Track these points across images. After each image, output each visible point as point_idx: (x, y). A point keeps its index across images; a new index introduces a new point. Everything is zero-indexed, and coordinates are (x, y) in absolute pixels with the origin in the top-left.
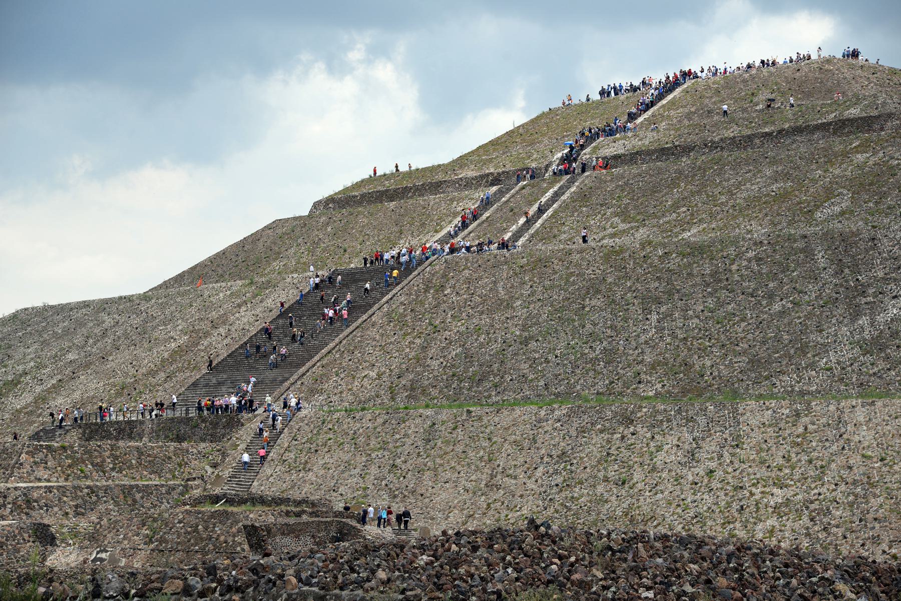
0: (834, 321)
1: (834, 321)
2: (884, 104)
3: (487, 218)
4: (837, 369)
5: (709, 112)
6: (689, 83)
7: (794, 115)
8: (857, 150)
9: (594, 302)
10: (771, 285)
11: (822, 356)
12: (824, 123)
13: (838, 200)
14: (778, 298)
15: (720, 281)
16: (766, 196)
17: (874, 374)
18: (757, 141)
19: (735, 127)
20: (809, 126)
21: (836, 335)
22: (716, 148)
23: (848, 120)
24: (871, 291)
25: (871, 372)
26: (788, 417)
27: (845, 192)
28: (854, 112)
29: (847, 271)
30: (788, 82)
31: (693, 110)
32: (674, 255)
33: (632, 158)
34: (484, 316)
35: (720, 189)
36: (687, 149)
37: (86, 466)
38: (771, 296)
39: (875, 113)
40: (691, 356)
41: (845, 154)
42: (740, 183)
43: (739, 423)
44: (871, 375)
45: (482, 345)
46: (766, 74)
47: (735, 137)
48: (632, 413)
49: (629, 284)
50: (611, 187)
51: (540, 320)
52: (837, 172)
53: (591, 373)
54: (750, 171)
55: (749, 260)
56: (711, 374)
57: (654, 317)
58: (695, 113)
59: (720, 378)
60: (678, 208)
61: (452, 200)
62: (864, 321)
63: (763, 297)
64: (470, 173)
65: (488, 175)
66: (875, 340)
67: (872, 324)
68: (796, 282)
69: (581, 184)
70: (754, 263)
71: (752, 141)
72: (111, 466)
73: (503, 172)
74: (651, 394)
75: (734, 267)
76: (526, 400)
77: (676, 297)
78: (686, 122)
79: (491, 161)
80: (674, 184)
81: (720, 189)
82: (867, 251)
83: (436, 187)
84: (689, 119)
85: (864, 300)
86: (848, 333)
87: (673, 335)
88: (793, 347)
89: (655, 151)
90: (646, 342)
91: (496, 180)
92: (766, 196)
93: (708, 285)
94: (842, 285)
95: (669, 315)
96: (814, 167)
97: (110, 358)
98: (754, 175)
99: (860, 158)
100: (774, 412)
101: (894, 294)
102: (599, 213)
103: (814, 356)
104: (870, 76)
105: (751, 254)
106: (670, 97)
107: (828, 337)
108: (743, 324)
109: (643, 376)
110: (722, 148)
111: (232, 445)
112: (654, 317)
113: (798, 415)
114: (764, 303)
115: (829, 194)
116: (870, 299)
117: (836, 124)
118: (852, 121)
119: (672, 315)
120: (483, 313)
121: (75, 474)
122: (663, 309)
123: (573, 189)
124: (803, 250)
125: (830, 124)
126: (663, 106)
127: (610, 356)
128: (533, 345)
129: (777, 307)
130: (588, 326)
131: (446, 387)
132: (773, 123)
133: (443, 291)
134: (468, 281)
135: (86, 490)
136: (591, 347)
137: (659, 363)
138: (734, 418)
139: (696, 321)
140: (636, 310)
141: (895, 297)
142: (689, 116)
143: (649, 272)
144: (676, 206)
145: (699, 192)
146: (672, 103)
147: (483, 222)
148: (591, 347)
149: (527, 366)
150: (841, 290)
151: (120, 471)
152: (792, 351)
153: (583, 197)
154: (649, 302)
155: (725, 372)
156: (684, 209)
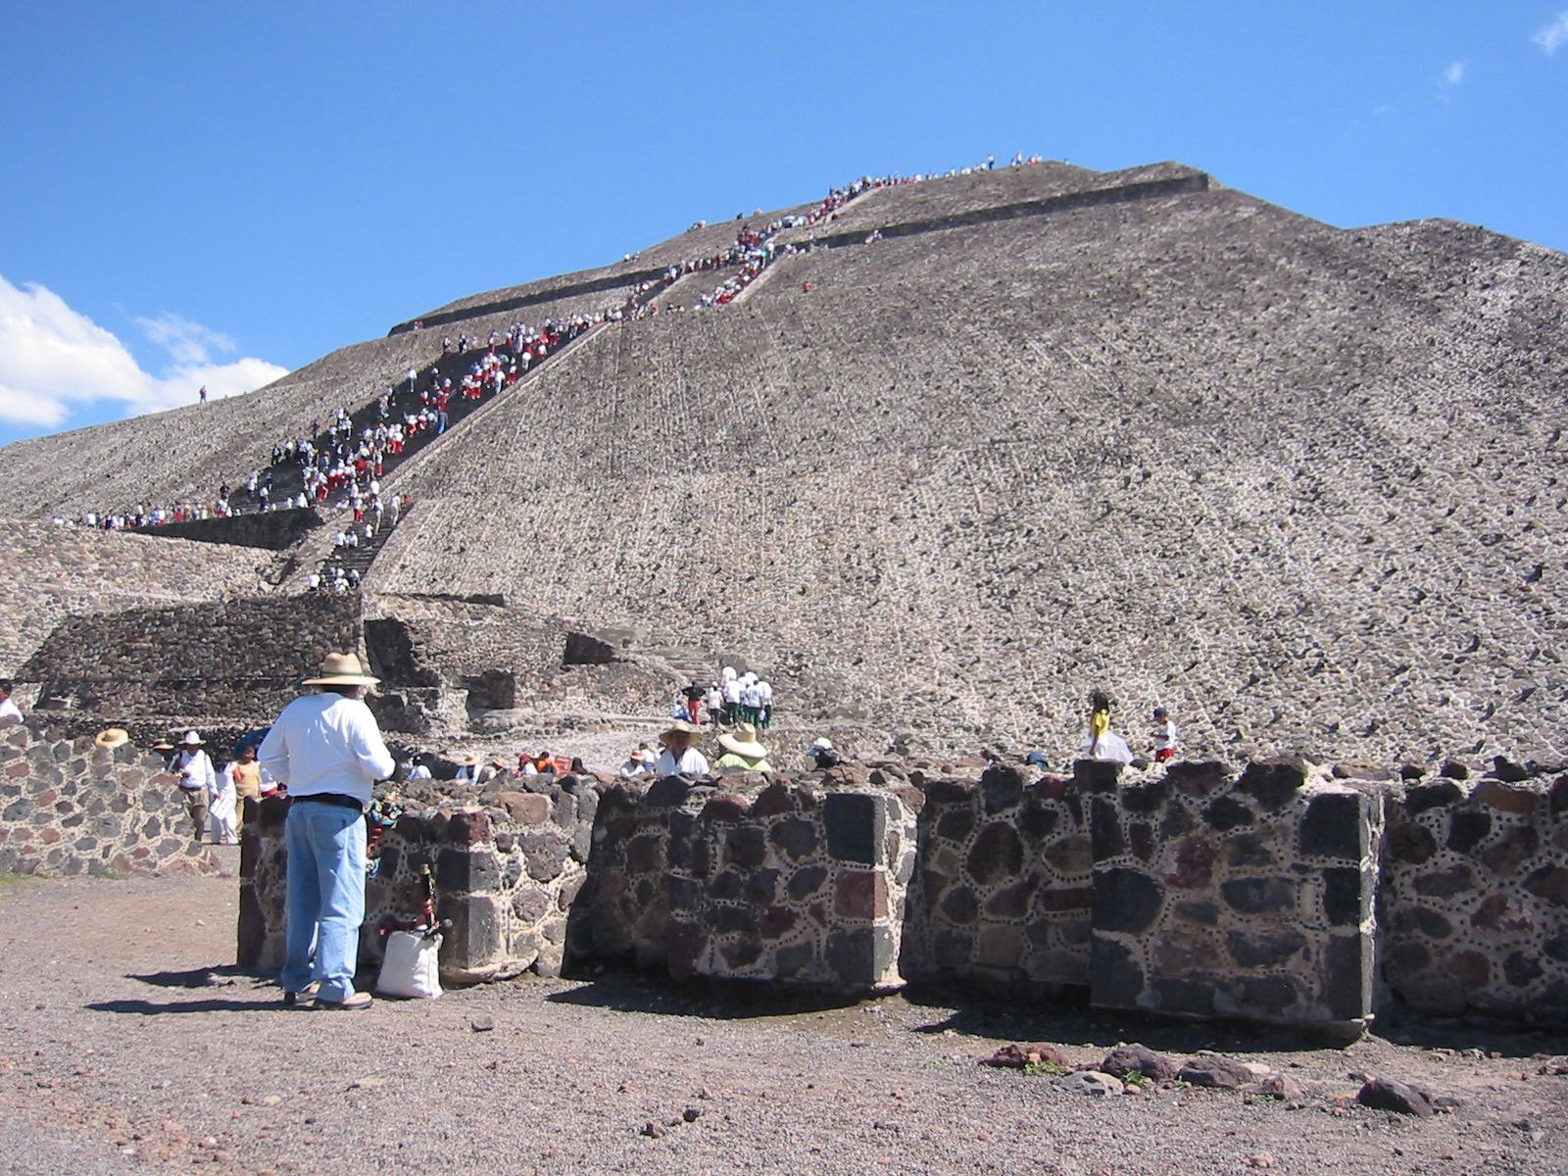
23: (1143, 184)
37: (50, 561)
45: (724, 405)
52: (1165, 230)
61: (588, 301)
72: (96, 567)
83: (564, 293)
93: (1109, 305)
95: (1065, 339)
97: (117, 476)
111: (306, 550)
121: (30, 573)
125: (1118, 189)
135: (45, 598)
140: (995, 341)
151: (112, 577)
154: (1014, 333)
155: (1242, 395)
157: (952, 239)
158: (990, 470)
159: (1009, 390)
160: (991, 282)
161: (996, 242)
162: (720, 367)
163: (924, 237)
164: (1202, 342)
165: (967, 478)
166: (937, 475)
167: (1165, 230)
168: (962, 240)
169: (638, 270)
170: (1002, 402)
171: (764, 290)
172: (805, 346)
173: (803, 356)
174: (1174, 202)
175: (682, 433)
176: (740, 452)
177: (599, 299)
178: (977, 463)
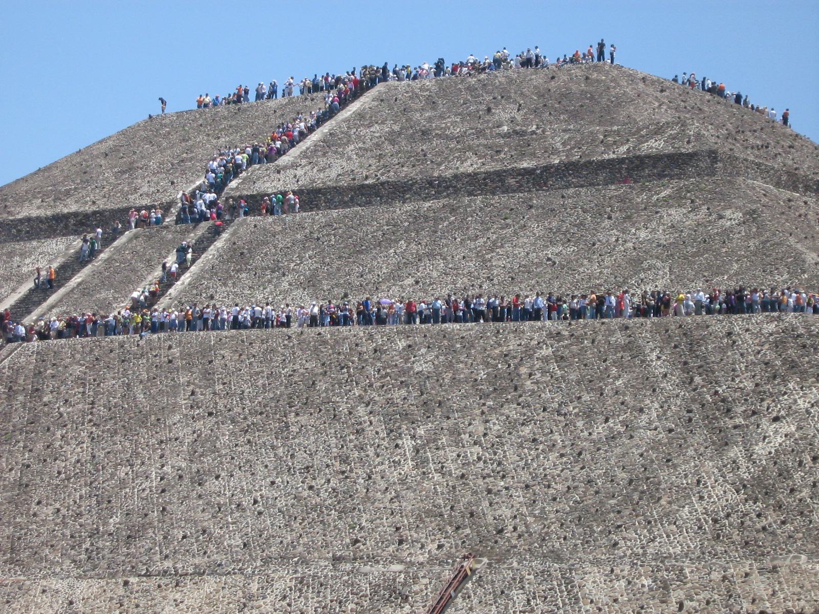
0: (691, 452)
1: (691, 452)
2: (698, 136)
3: (80, 284)
4: (707, 522)
5: (424, 133)
6: (380, 87)
7: (564, 144)
8: (667, 202)
9: (303, 419)
10: (586, 397)
11: (682, 502)
12: (613, 160)
13: (650, 275)
14: (601, 418)
15: (504, 390)
16: (538, 265)
17: (764, 528)
18: (512, 181)
19: (475, 158)
20: (590, 163)
21: (697, 473)
22: (447, 188)
23: (648, 157)
24: (740, 409)
25: (758, 526)
26: (651, 589)
27: (659, 264)
28: (655, 145)
29: (698, 379)
30: (540, 95)
31: (396, 128)
32: (423, 350)
33: (312, 198)
34: (117, 438)
35: (462, 252)
36: (398, 191)
38: (589, 415)
39: (687, 149)
40: (478, 503)
41: (653, 210)
42: (494, 243)
43: (577, 599)
44: (758, 531)
45: (123, 484)
46: (503, 80)
47: (476, 174)
48: (404, 584)
49: (357, 392)
50: (282, 242)
51: (218, 445)
52: (643, 234)
53: (318, 528)
54: (508, 226)
55: (545, 360)
56: (515, 529)
57: (408, 443)
58: (400, 134)
59: (531, 535)
60: (400, 278)
61: (11, 255)
62: (735, 452)
63: (577, 415)
64: (32, 210)
65: (66, 217)
66: (758, 481)
67: (749, 458)
68: (624, 395)
69: (233, 234)
70: (553, 367)
71: (502, 181)
73: (95, 213)
74: (421, 559)
75: (524, 370)
76: (215, 569)
77: (438, 413)
78: (388, 148)
79: (68, 193)
80: (386, 241)
81: (462, 252)
82: (723, 350)
84: (393, 142)
85: (730, 423)
86: (716, 471)
87: (441, 471)
88: (635, 490)
89: (350, 188)
90: (403, 481)
91: (79, 223)
92: (538, 265)
94: (694, 400)
95: (432, 440)
96: (607, 223)
98: (515, 233)
99: (675, 214)
100: (629, 583)
101: (775, 414)
102: (270, 282)
103: (670, 503)
104: (658, 94)
105: (546, 351)
106: (355, 107)
107: (686, 476)
108: (553, 456)
109: (405, 533)
110: (457, 191)
112: (408, 443)
113: (665, 586)
114: (580, 424)
115: (636, 263)
116: (739, 421)
117: (631, 162)
118: (656, 159)
119: (435, 440)
120: (116, 432)
122: (421, 431)
123: (219, 244)
124: (627, 347)
125: (621, 161)
126: (347, 120)
127: (345, 501)
128: (212, 485)
129: (600, 430)
130: (300, 455)
131: (73, 548)
132: (533, 155)
133: (40, 397)
134: (81, 381)
136: (311, 488)
137: (428, 513)
138: (569, 592)
139: (477, 449)
140: (375, 429)
141: (776, 419)
142: (392, 138)
143: (387, 374)
144: (395, 276)
145: (431, 255)
146: (360, 115)
147: (72, 290)
148: (311, 488)
149: (207, 516)
150: (694, 407)
152: (636, 497)
153: (238, 256)
154: (396, 419)
155: (536, 527)
156: (410, 281)
157: (426, 219)
158: (306, 598)
159: (367, 499)
160: (402, 344)
161: (471, 232)
162: (127, 430)
163: (402, 210)
164: (538, 456)
165: (289, 605)
166: (268, 600)
167: (643, 234)
168: (437, 220)
169: (74, 208)
170: (356, 512)
171: (212, 271)
172: (210, 414)
173: (204, 426)
174: (667, 192)
175: (80, 515)
176: (128, 544)
177: (23, 255)
178: (300, 590)
